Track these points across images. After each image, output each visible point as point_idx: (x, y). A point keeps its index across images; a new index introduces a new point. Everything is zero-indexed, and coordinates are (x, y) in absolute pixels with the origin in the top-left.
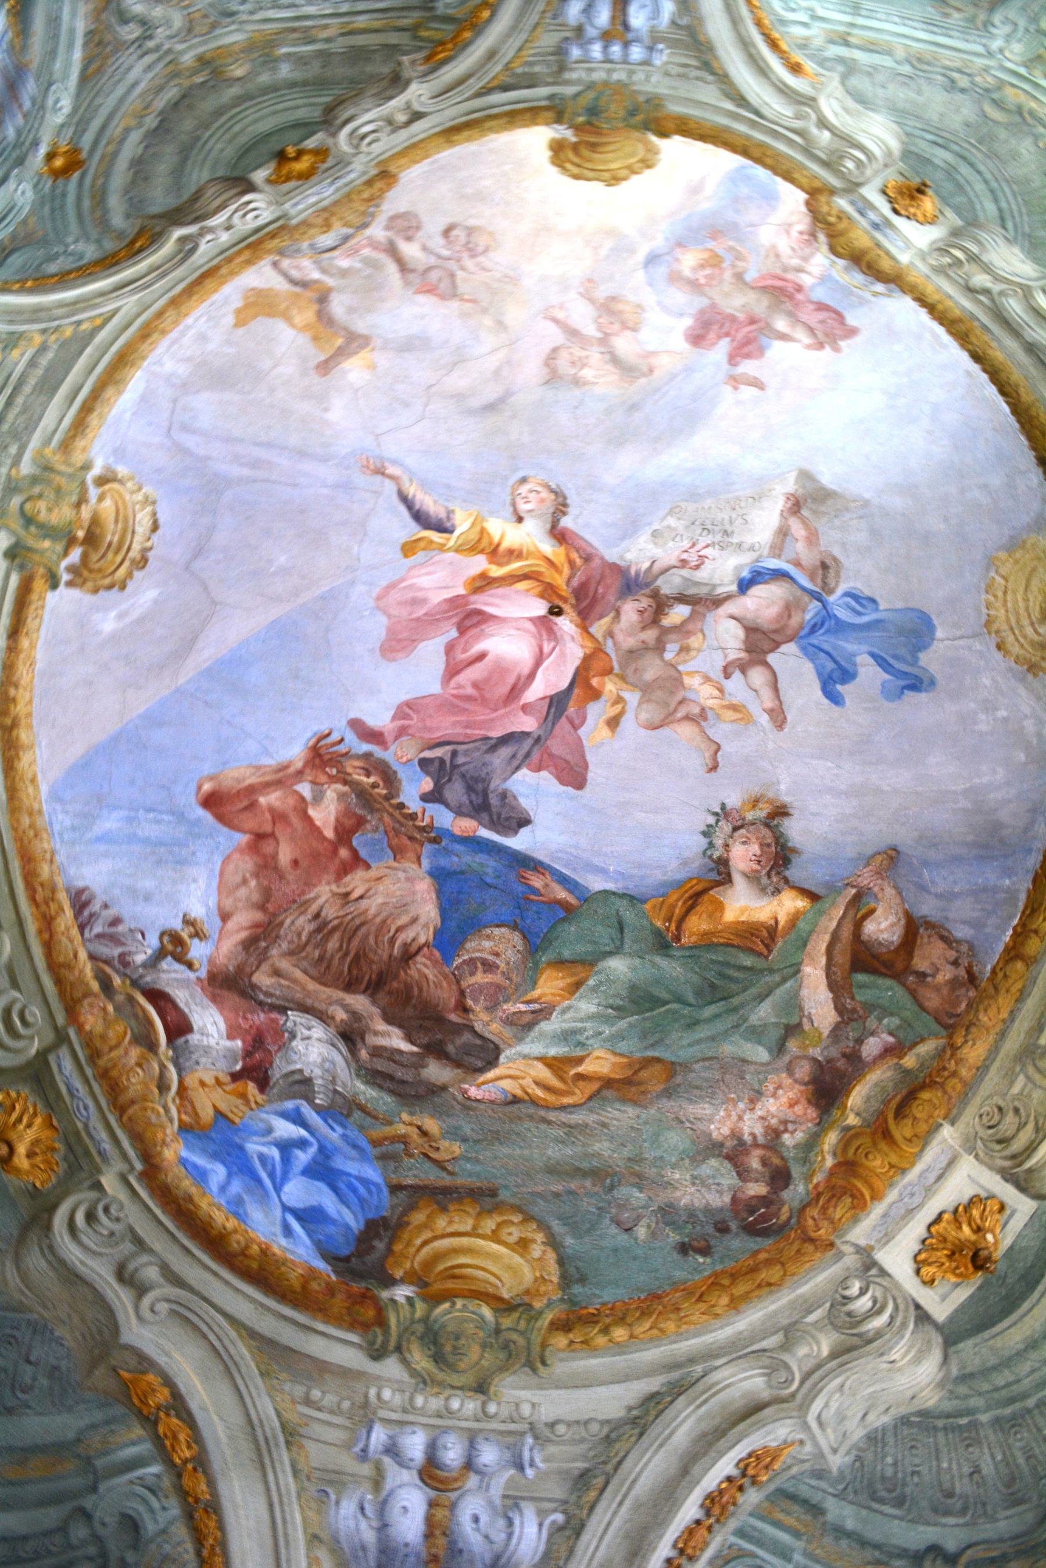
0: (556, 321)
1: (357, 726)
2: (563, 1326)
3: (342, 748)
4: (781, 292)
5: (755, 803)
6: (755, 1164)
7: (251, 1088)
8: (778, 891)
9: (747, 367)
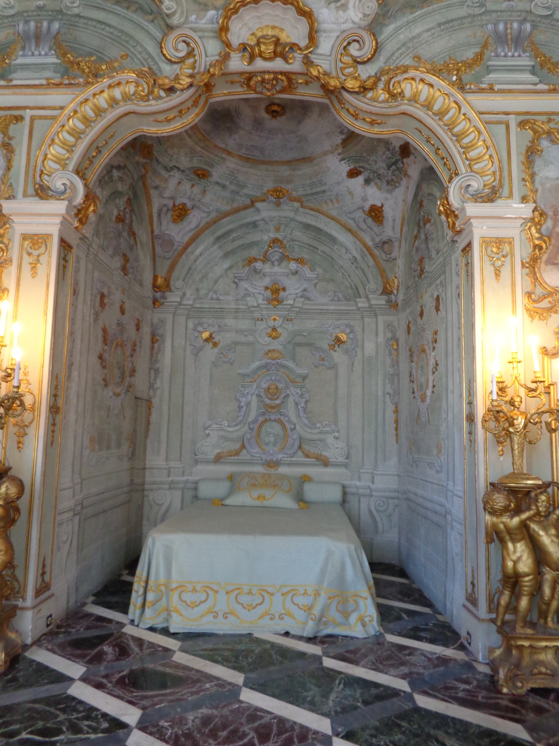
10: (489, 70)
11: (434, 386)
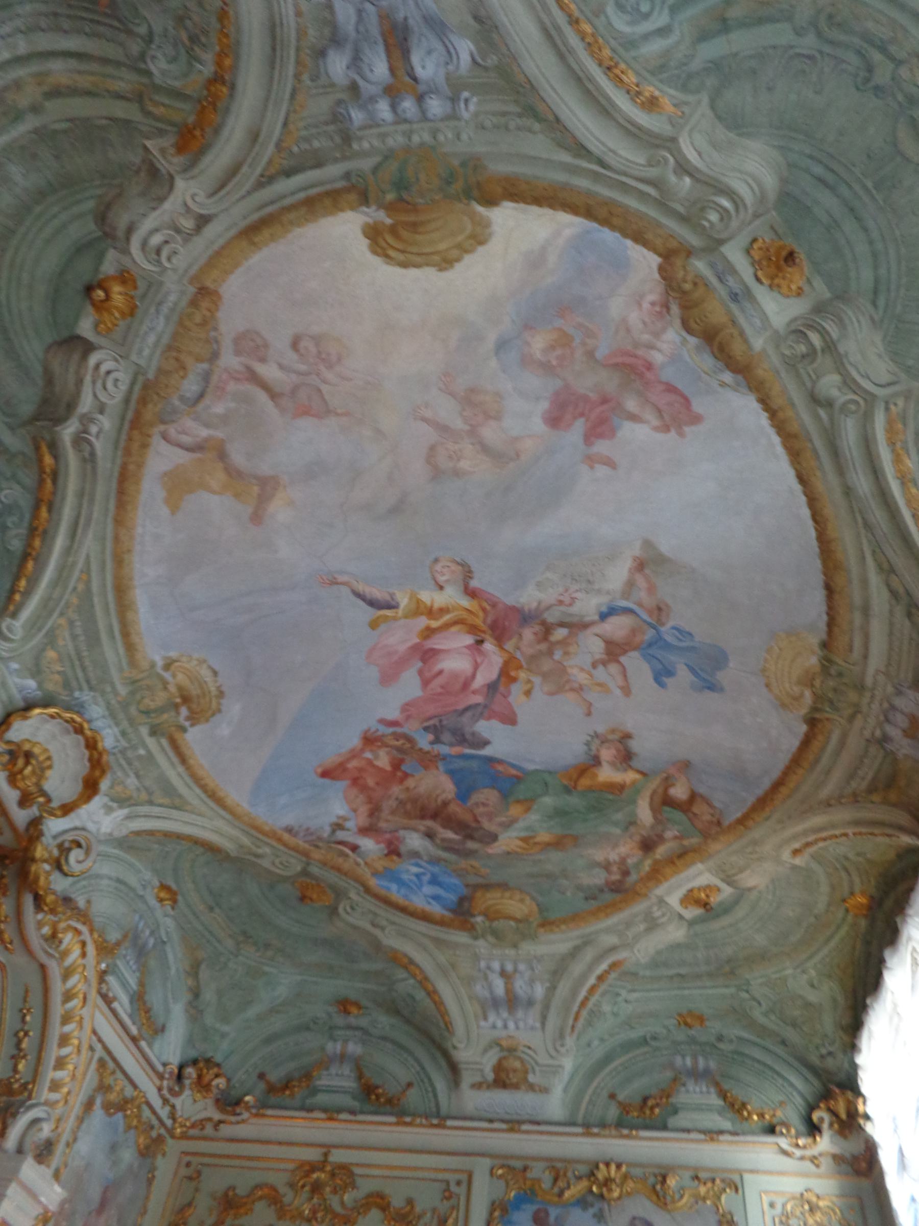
0: (424, 419)
1: (383, 721)
2: (542, 925)
3: (379, 733)
4: (633, 369)
5: (613, 731)
6: (615, 869)
7: (395, 858)
8: (625, 770)
9: (602, 447)
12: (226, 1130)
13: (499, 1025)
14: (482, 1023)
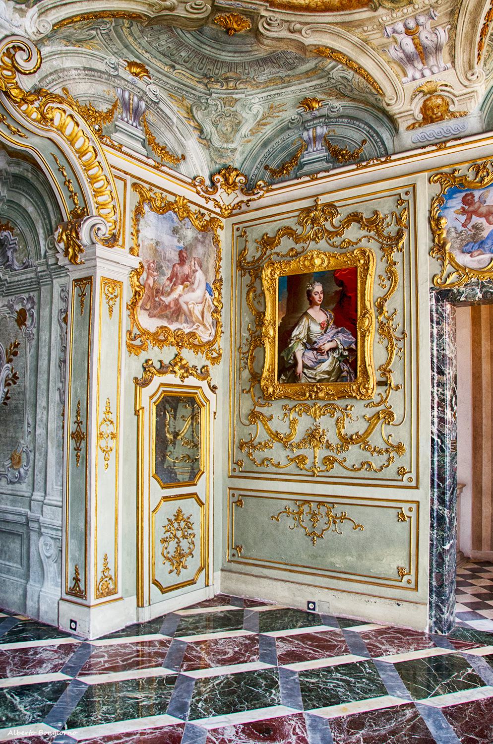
10: (116, 129)
11: (7, 398)
12: (253, 205)
13: (417, 77)
14: (404, 79)
